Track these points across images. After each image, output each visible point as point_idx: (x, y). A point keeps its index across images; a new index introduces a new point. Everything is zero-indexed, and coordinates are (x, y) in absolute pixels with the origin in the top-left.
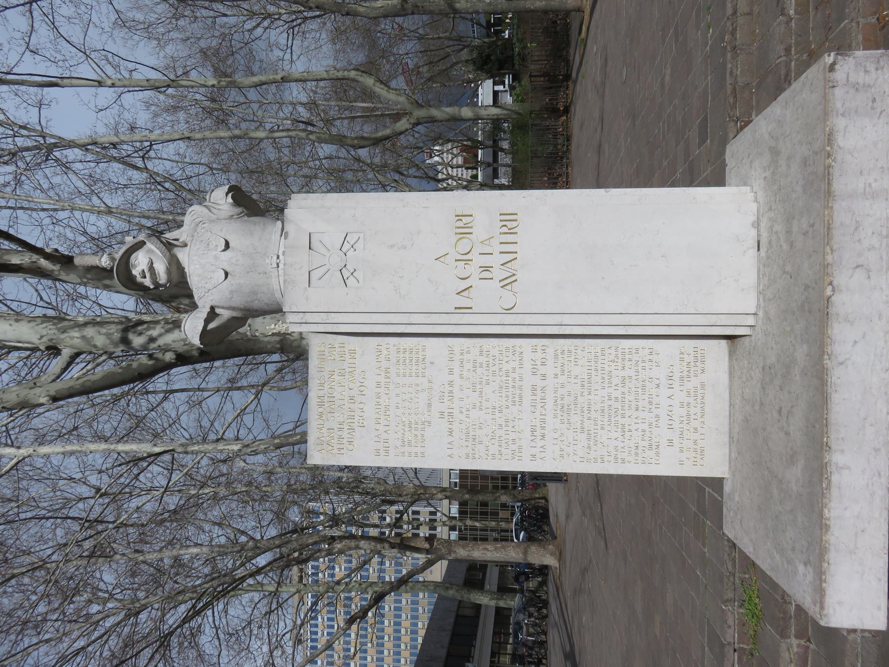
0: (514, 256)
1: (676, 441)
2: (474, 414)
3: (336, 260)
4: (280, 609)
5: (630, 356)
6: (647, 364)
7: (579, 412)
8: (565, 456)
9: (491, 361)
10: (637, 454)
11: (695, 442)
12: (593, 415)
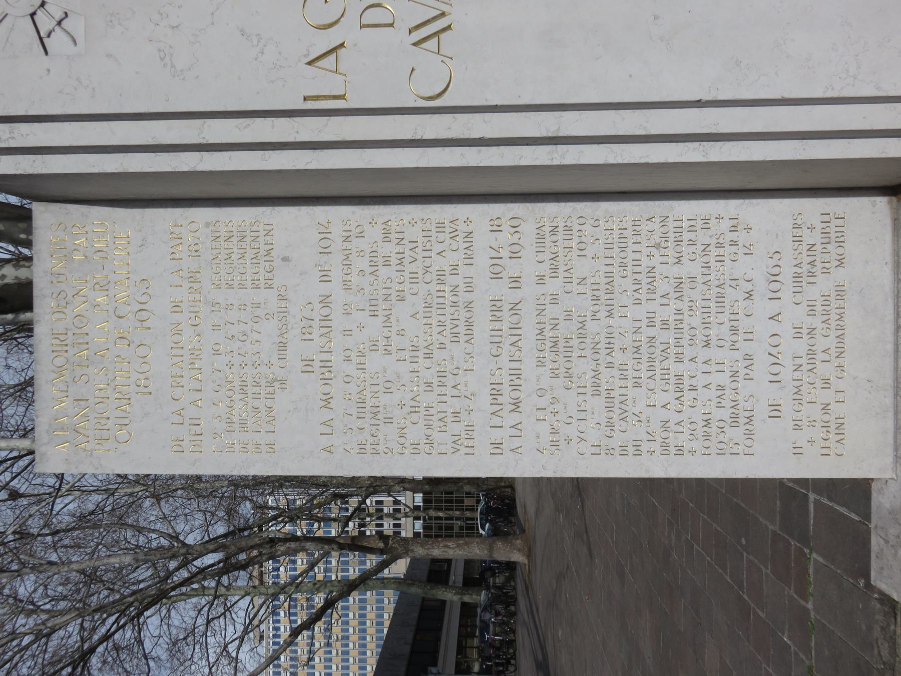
1: (787, 408)
2: (375, 362)
5: (692, 236)
6: (727, 250)
7: (588, 352)
8: (562, 443)
9: (408, 253)
10: (707, 437)
11: (826, 407)
12: (618, 357)
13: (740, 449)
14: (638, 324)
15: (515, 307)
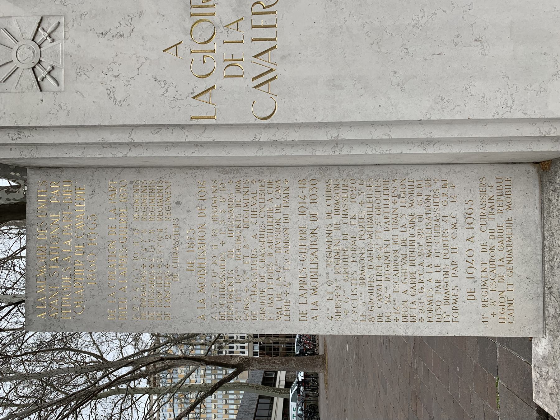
0: (273, 43)
1: (478, 295)
2: (231, 264)
5: (419, 190)
6: (442, 199)
7: (357, 259)
8: (343, 314)
9: (251, 200)
11: (501, 294)
13: (451, 318)
14: (387, 243)
15: (313, 232)
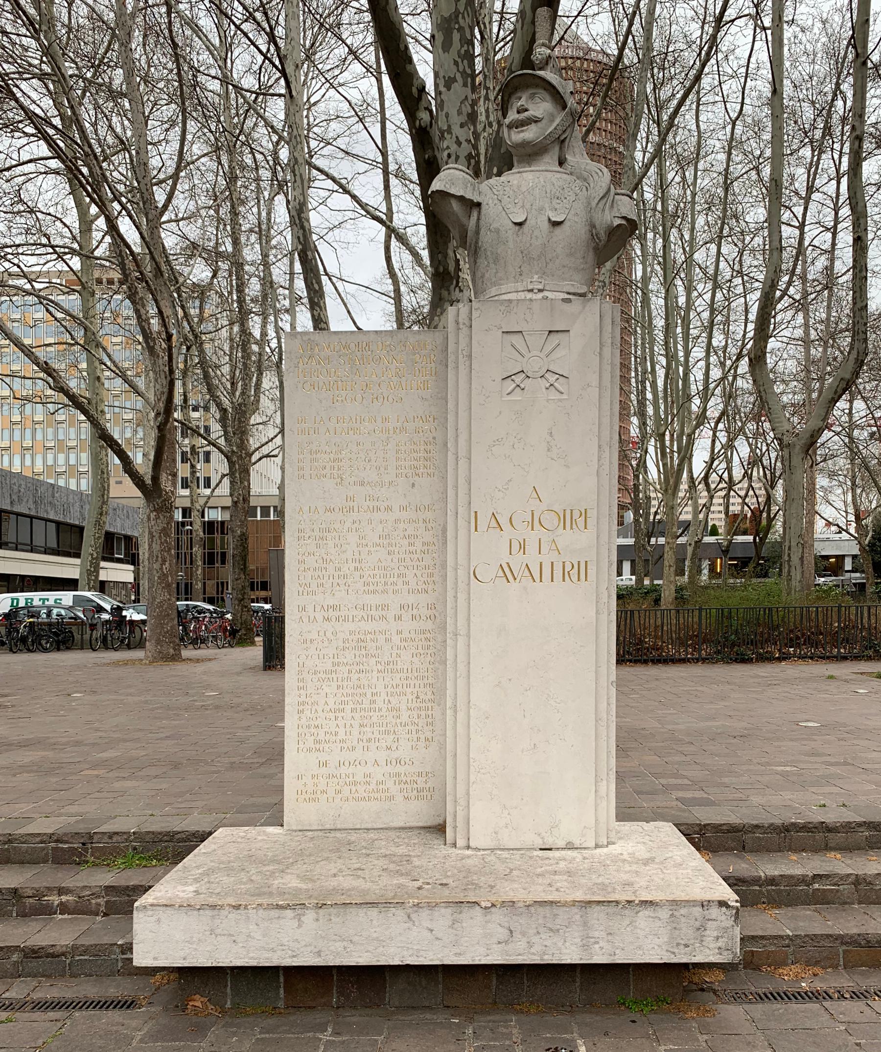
1: (324, 770)
3: (534, 365)
4: (55, 256)
7: (358, 659)
8: (305, 646)
9: (416, 556)
10: (308, 727)
12: (355, 676)
13: (301, 746)
14: (373, 687)
15: (383, 618)
